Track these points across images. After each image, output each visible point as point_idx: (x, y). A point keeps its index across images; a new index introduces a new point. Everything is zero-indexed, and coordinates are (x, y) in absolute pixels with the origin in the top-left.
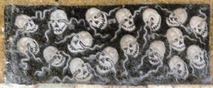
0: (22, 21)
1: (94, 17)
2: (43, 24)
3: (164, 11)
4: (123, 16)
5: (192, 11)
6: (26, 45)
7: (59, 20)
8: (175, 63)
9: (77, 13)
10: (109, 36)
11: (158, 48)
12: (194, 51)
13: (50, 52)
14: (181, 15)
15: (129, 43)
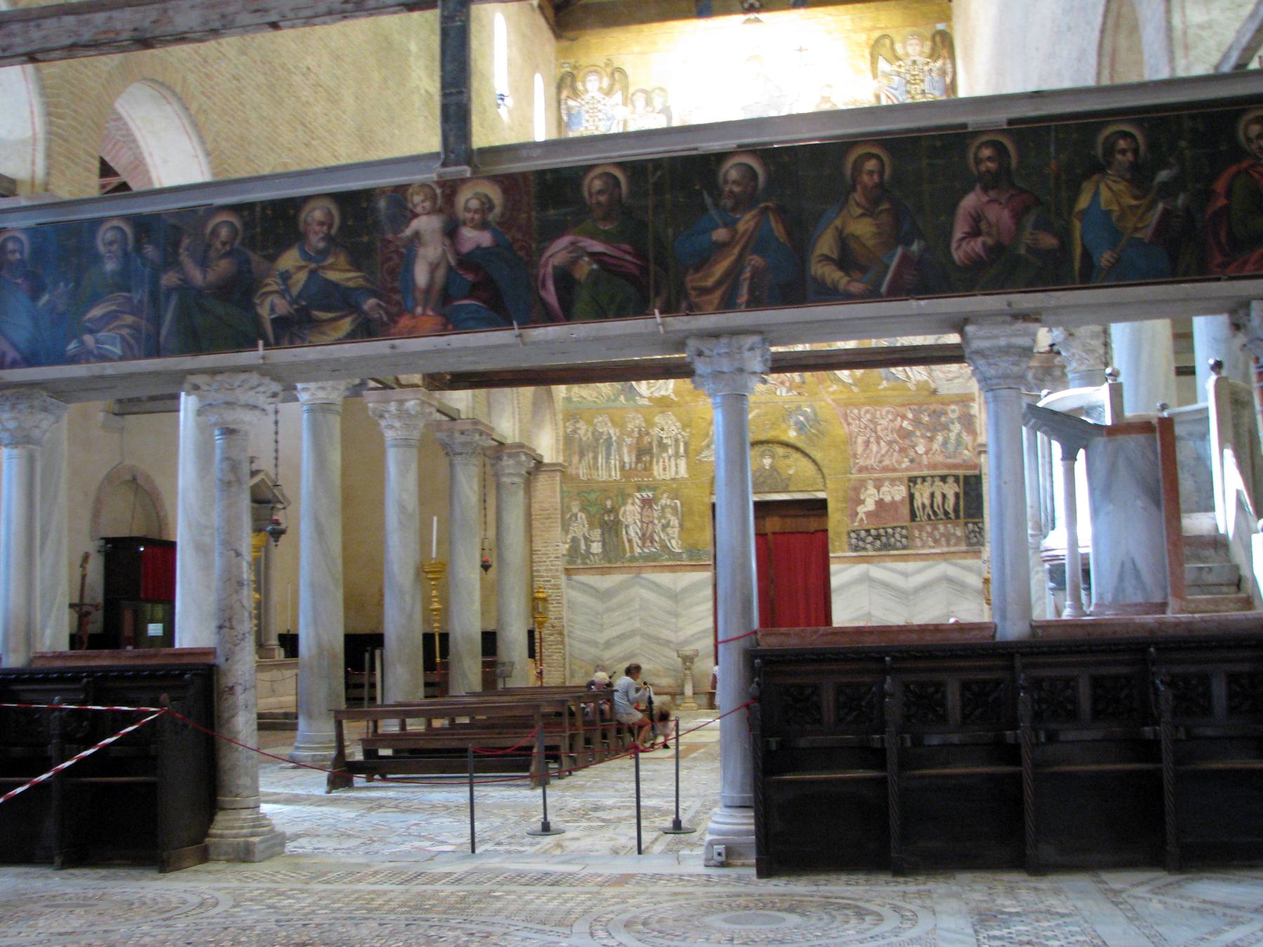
0: (853, 535)
1: (873, 532)
2: (858, 535)
3: (894, 528)
4: (882, 531)
5: (902, 528)
6: (854, 541)
7: (863, 534)
8: (898, 544)
9: (868, 531)
10: (878, 537)
11: (892, 540)
12: (904, 540)
13: (861, 543)
14: (899, 530)
15: (884, 539)
